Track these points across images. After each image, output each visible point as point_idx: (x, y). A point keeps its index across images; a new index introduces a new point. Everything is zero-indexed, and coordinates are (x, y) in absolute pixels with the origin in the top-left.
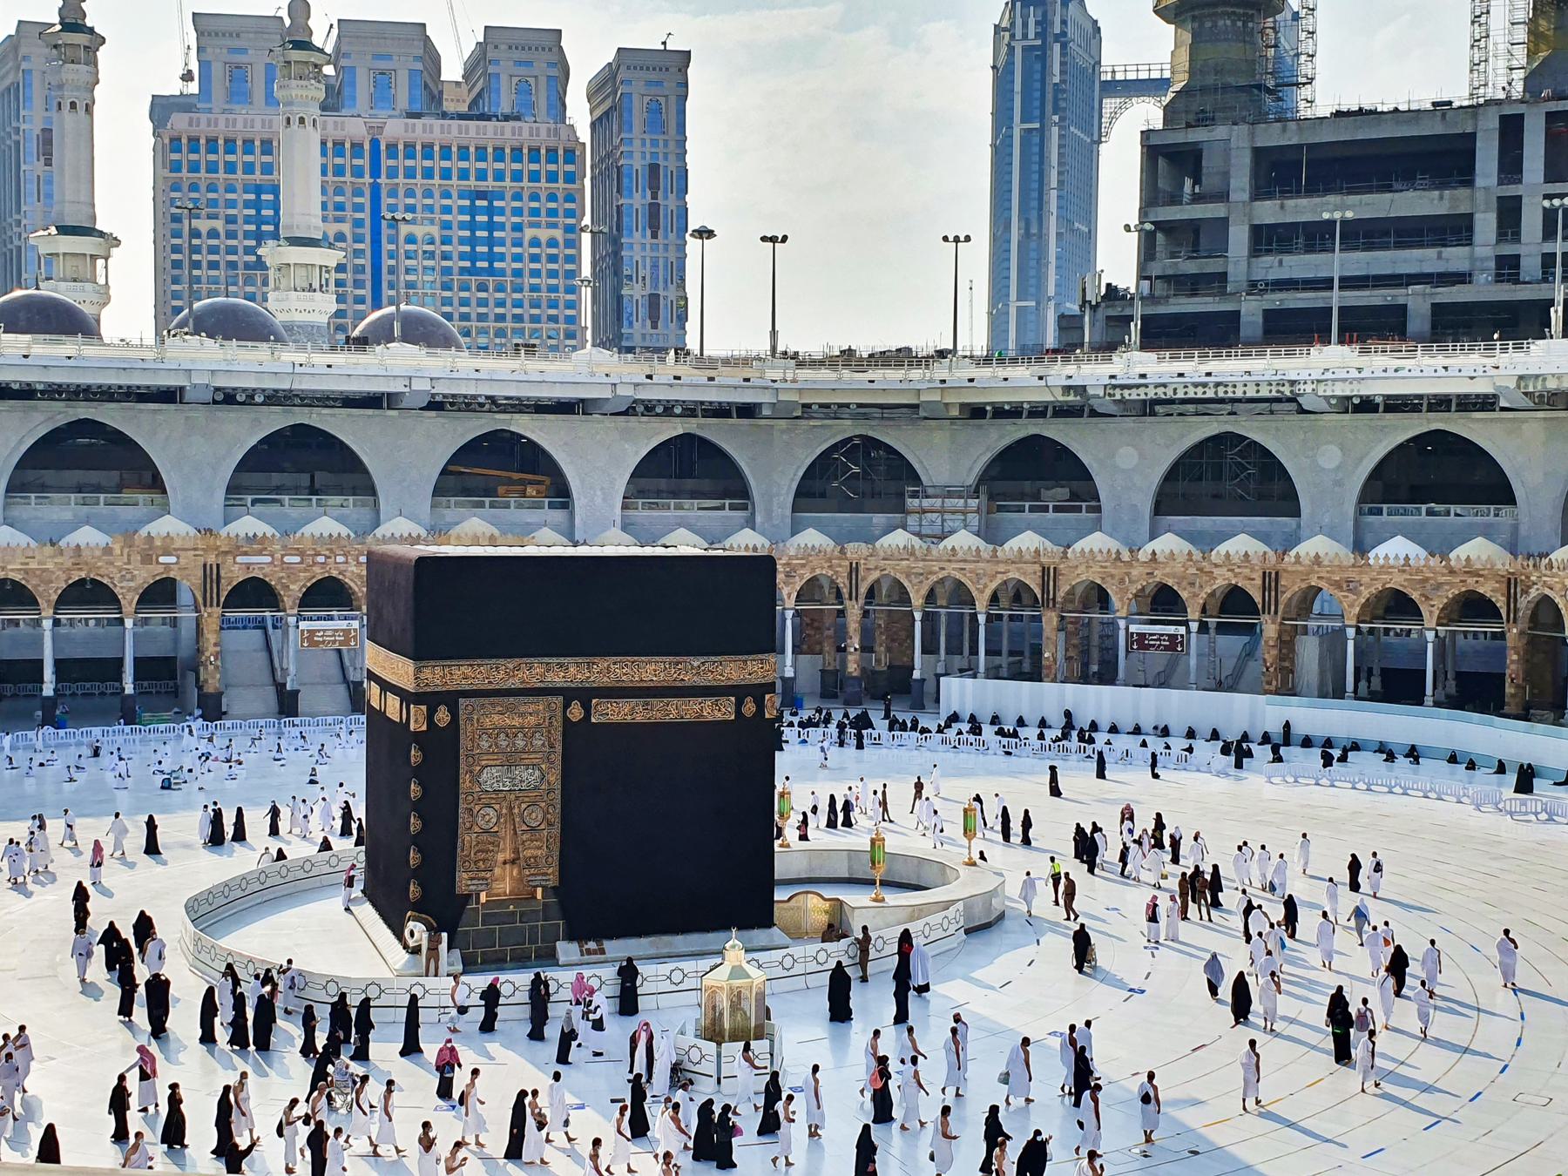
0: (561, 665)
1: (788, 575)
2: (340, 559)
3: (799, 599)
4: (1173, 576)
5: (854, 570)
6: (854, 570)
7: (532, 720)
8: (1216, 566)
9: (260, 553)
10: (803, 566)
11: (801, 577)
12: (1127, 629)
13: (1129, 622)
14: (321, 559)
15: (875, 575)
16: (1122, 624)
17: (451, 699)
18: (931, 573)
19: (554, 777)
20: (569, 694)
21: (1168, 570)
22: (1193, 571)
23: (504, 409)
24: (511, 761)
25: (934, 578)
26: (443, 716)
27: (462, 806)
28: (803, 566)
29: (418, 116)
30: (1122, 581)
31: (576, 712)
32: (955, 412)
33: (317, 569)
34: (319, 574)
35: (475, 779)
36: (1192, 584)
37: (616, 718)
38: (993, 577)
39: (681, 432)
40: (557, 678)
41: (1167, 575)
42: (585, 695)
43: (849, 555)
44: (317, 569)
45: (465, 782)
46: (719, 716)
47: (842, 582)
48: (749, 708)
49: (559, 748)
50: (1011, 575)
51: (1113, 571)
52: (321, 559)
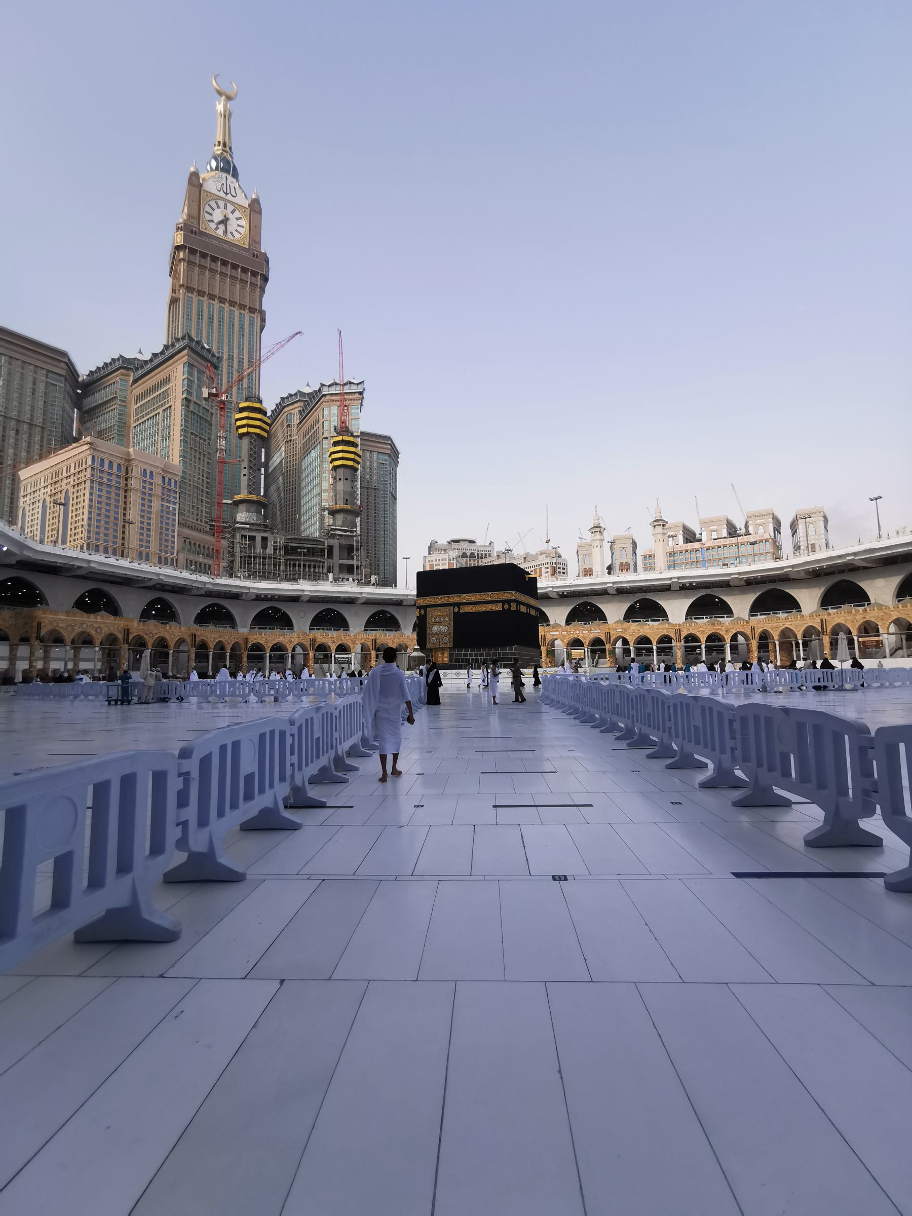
0: (452, 597)
1: (726, 632)
2: (577, 632)
3: (731, 641)
4: (874, 617)
5: (753, 629)
6: (753, 629)
7: (445, 613)
8: (892, 611)
9: (555, 631)
10: (732, 628)
11: (732, 632)
12: (858, 640)
13: (859, 637)
14: (572, 632)
15: (761, 630)
16: (855, 638)
17: (425, 607)
18: (781, 627)
19: (452, 630)
20: (454, 605)
21: (871, 615)
22: (883, 614)
23: (645, 591)
24: (440, 624)
25: (781, 629)
26: (423, 612)
27: (427, 637)
28: (732, 628)
29: (716, 539)
30: (853, 622)
31: (456, 610)
32: (802, 575)
33: (571, 635)
34: (572, 637)
35: (431, 630)
36: (882, 619)
37: (467, 611)
38: (802, 626)
39: (704, 593)
40: (452, 600)
41: (872, 617)
42: (459, 605)
43: (750, 624)
44: (571, 635)
45: (428, 631)
46: (497, 609)
47: (749, 633)
48: (506, 607)
49: (452, 620)
50: (809, 624)
51: (848, 618)
52: (572, 632)
